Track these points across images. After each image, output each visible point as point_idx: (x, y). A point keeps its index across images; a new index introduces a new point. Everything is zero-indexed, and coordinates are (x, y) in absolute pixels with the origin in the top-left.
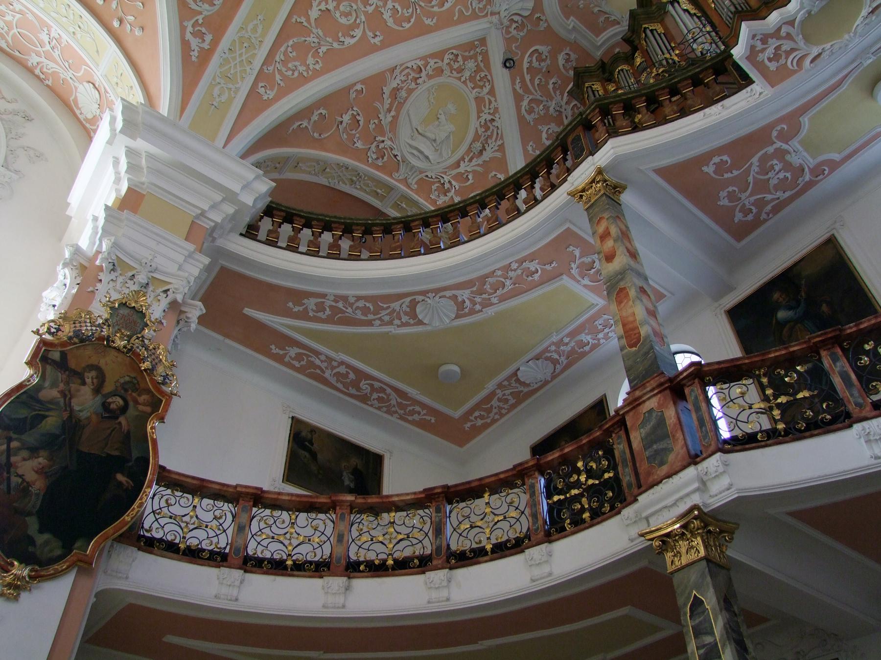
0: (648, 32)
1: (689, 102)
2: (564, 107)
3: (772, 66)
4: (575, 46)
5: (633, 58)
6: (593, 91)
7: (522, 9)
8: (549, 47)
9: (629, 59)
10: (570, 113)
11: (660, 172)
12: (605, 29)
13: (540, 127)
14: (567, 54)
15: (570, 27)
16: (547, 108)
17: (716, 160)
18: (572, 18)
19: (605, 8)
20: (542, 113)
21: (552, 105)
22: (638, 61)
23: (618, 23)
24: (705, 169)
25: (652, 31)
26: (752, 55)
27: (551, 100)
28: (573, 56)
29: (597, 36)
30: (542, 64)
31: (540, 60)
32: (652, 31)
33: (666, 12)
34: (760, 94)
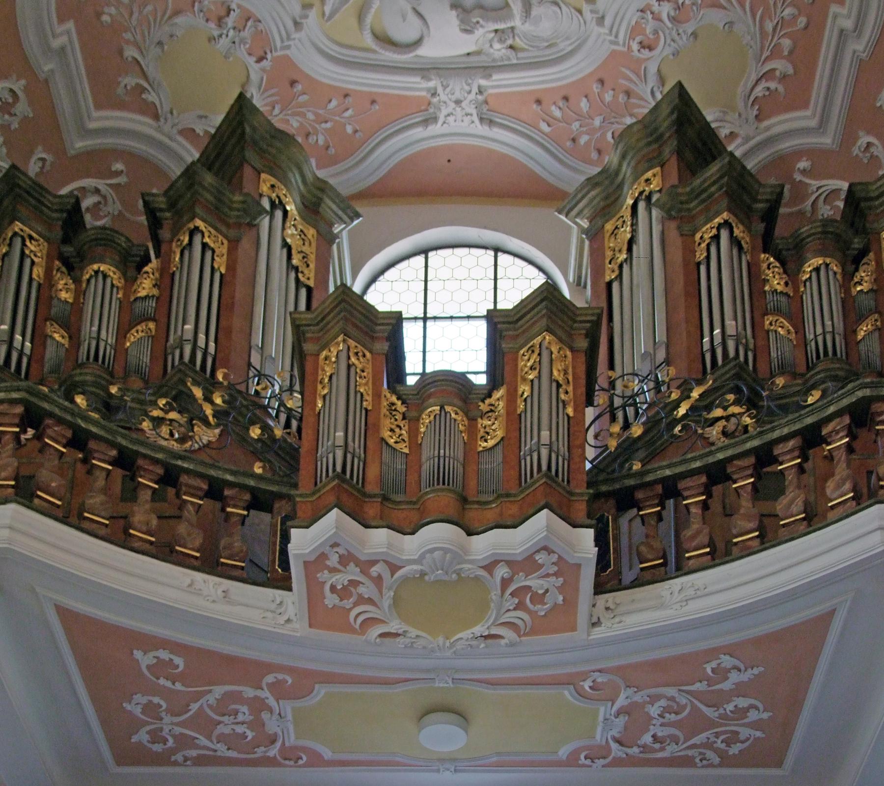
0: (197, 239)
1: (182, 529)
3: (331, 600)
6: (23, 255)
9: (133, 264)
11: (64, 613)
12: (121, 106)
25: (205, 246)
29: (99, 106)
32: (205, 246)
33: (253, 226)
34: (288, 621)
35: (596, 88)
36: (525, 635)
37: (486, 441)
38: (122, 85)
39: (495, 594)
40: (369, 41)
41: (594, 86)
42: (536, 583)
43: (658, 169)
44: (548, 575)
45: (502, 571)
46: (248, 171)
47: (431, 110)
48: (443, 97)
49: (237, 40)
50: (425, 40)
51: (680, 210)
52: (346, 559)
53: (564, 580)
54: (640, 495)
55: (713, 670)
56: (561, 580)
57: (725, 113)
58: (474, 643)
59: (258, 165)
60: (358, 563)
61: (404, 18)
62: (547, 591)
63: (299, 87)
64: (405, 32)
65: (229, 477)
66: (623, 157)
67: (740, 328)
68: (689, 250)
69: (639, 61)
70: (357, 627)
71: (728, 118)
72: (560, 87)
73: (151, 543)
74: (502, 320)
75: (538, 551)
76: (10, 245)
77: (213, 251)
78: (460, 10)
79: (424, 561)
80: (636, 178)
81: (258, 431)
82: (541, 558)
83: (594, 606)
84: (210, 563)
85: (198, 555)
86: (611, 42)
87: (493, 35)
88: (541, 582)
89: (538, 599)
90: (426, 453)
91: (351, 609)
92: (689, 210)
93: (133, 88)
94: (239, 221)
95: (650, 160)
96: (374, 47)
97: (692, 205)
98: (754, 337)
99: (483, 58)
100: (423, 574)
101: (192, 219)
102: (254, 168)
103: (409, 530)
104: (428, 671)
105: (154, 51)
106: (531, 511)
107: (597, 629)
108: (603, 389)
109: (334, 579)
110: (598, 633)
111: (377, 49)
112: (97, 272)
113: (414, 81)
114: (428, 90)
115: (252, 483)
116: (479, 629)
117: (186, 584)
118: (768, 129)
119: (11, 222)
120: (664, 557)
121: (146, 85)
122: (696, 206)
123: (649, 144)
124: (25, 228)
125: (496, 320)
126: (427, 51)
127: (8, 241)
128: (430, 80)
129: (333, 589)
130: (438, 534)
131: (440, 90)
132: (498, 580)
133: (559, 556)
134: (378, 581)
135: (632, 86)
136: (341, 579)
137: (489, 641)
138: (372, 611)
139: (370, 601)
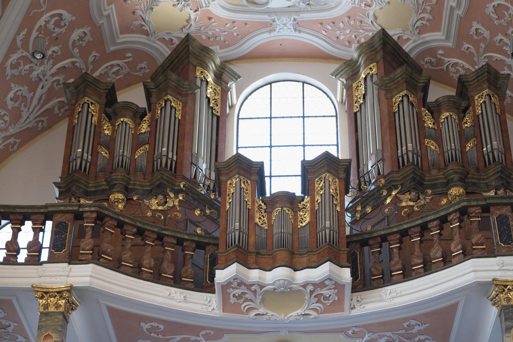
0: (168, 103)
2: (46, 78)
3: (233, 300)
4: (97, 31)
5: (142, 118)
8: (74, 18)
10: (48, 84)
12: (133, 32)
13: (12, 85)
14: (84, 32)
15: (105, 13)
16: (31, 70)
17: (155, 324)
19: (147, 18)
20: (23, 73)
21: (38, 71)
22: (144, 127)
23: (148, 35)
24: (142, 324)
26: (227, 286)
27: (40, 65)
28: (88, 38)
29: (122, 33)
30: (57, 30)
31: (57, 24)
32: (172, 107)
35: (346, 19)
36: (321, 313)
37: (302, 223)
39: (307, 297)
41: (346, 19)
42: (325, 292)
43: (375, 63)
44: (331, 289)
45: (310, 288)
46: (191, 67)
51: (385, 87)
52: (240, 284)
53: (338, 291)
54: (371, 242)
55: (407, 325)
56: (336, 291)
57: (404, 31)
58: (298, 317)
59: (195, 64)
60: (245, 285)
62: (330, 295)
63: (213, 20)
65: (186, 237)
66: (359, 56)
67: (414, 146)
68: (390, 106)
70: (245, 311)
71: (406, 33)
73: (151, 273)
74: (307, 165)
75: (326, 280)
76: (82, 107)
77: (176, 109)
79: (275, 284)
81: (199, 212)
82: (327, 282)
83: (352, 300)
84: (177, 282)
85: (172, 277)
88: (327, 292)
89: (326, 298)
90: (276, 230)
91: (242, 304)
92: (389, 87)
93: (138, 25)
94: (186, 93)
95: (372, 59)
97: (391, 85)
98: (421, 150)
100: (275, 289)
101: (166, 95)
103: (269, 269)
104: (277, 328)
106: (322, 262)
107: (354, 311)
108: (353, 188)
109: (235, 292)
110: (354, 313)
112: (122, 122)
114: (271, 20)
115: (196, 239)
116: (300, 311)
117: (168, 294)
118: (424, 38)
119: (84, 96)
120: (383, 274)
121: (144, 23)
123: (371, 51)
124: (89, 99)
125: (305, 165)
127: (81, 106)
129: (234, 296)
130: (280, 273)
131: (276, 20)
132: (309, 291)
133: (336, 282)
134: (255, 292)
135: (363, 19)
136: (238, 292)
137: (305, 316)
138: (251, 304)
139: (251, 300)
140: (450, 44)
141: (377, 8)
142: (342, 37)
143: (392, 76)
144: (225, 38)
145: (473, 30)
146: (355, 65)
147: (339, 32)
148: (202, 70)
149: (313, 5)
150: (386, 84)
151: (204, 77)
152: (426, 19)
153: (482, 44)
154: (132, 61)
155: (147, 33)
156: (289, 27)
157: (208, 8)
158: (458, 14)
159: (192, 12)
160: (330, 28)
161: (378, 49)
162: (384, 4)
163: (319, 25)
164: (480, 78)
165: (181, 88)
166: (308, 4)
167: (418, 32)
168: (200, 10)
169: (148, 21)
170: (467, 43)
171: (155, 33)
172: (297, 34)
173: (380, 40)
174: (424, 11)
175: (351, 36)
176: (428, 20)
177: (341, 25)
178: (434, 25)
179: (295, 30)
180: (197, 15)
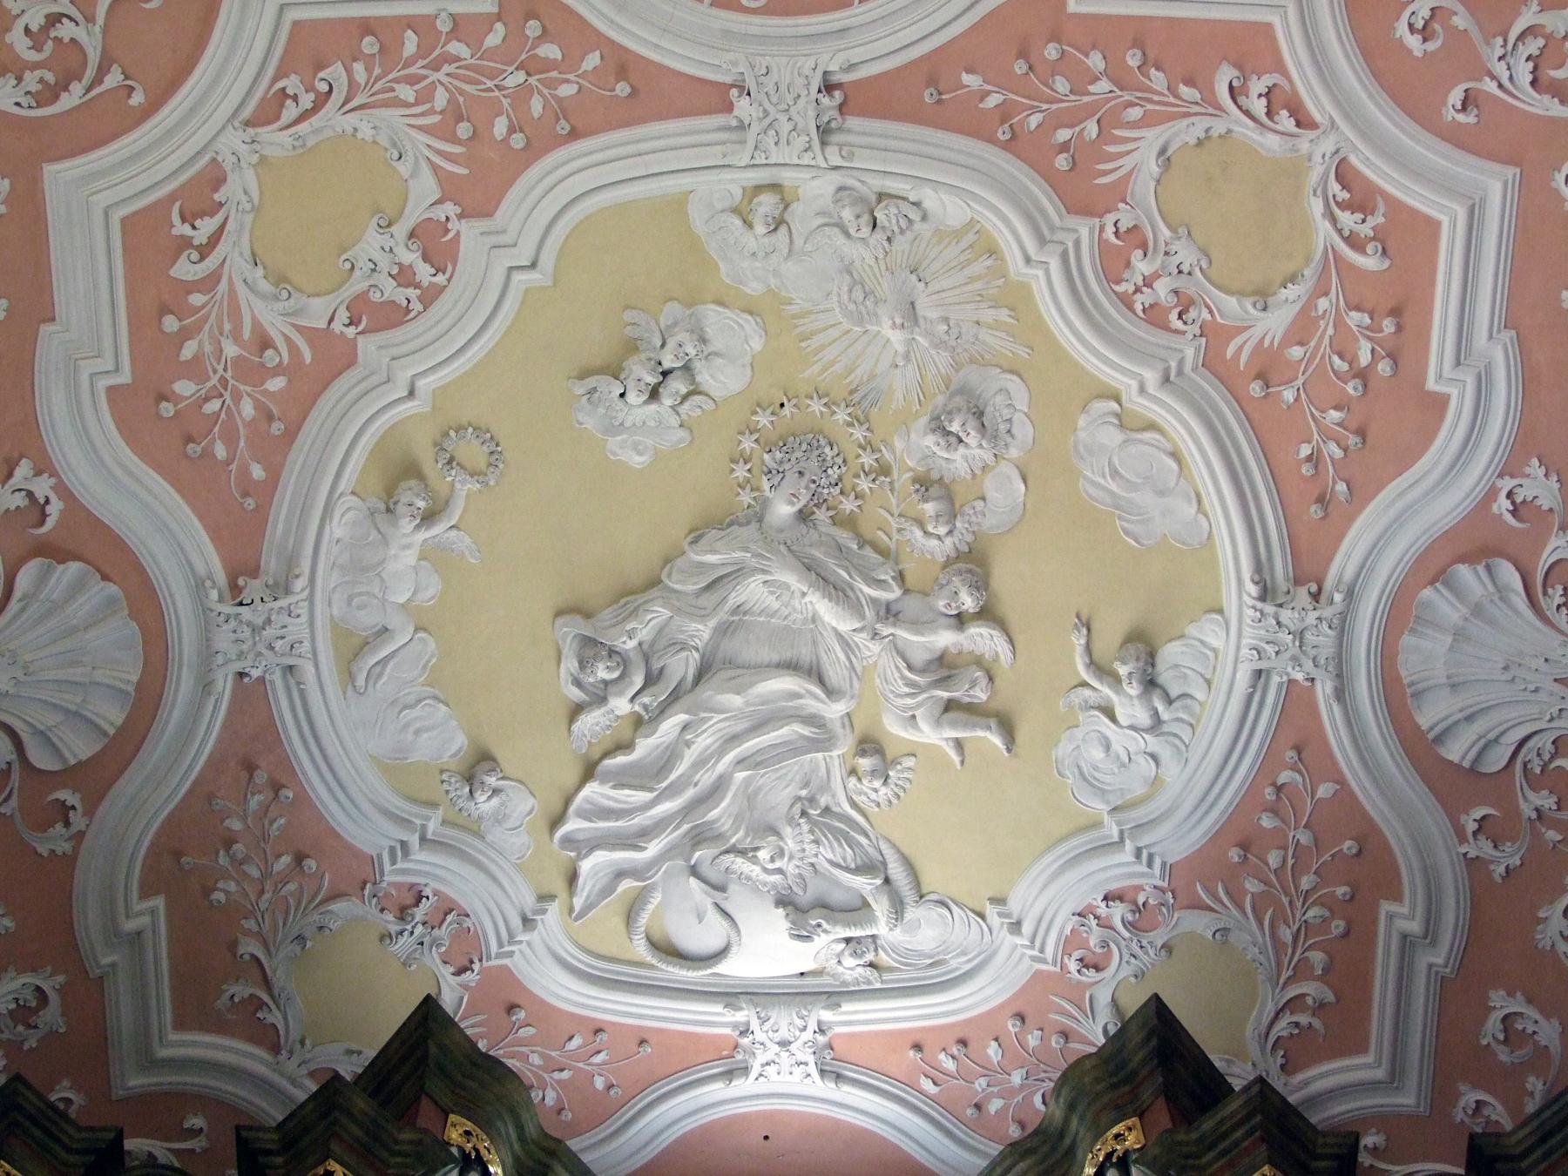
7: (43, 736)
18: (159, 902)
19: (279, 978)
23: (275, 1049)
29: (180, 1025)
35: (1012, 1027)
38: (227, 995)
40: (641, 950)
41: (1010, 1025)
47: (739, 1057)
48: (760, 1036)
49: (427, 940)
50: (734, 949)
59: (446, 1101)
61: (700, 918)
63: (522, 1015)
64: (700, 935)
66: (1071, 1107)
69: (1081, 987)
72: (953, 1025)
78: (790, 908)
80: (1098, 1134)
86: (1033, 959)
87: (843, 945)
93: (243, 1001)
95: (1118, 1107)
96: (649, 959)
99: (826, 980)
102: (436, 1103)
105: (288, 949)
111: (649, 959)
113: (716, 1008)
114: (735, 1026)
118: (1306, 1083)
121: (265, 997)
122: (1216, 1159)
123: (1114, 1086)
126: (734, 968)
128: (741, 1009)
131: (755, 1025)
140: (1406, 1100)
141: (1126, 971)
142: (995, 1105)
143: (1208, 1124)
144: (559, 1098)
145: (1493, 1024)
146: (1054, 1149)
147: (983, 1082)
148: (469, 1126)
149: (891, 969)
150: (1187, 1157)
151: (477, 1151)
152: (1309, 1001)
153: (1532, 1079)
154: (205, 1151)
155: (271, 1040)
156: (801, 1057)
157: (506, 961)
158: (1430, 966)
159: (446, 972)
160: (950, 1065)
161: (1144, 1072)
162: (1151, 952)
163: (911, 1053)
164: (1553, 1142)
165: (386, 1155)
166: (871, 965)
167: (1280, 1061)
168: (476, 967)
169: (283, 989)
170: (1476, 1086)
171: (302, 1042)
172: (827, 1089)
173: (1148, 1039)
174: (1301, 971)
175: (1028, 1099)
176: (1320, 1008)
177: (993, 1051)
178: (1342, 1027)
179: (822, 1072)
180: (465, 987)
